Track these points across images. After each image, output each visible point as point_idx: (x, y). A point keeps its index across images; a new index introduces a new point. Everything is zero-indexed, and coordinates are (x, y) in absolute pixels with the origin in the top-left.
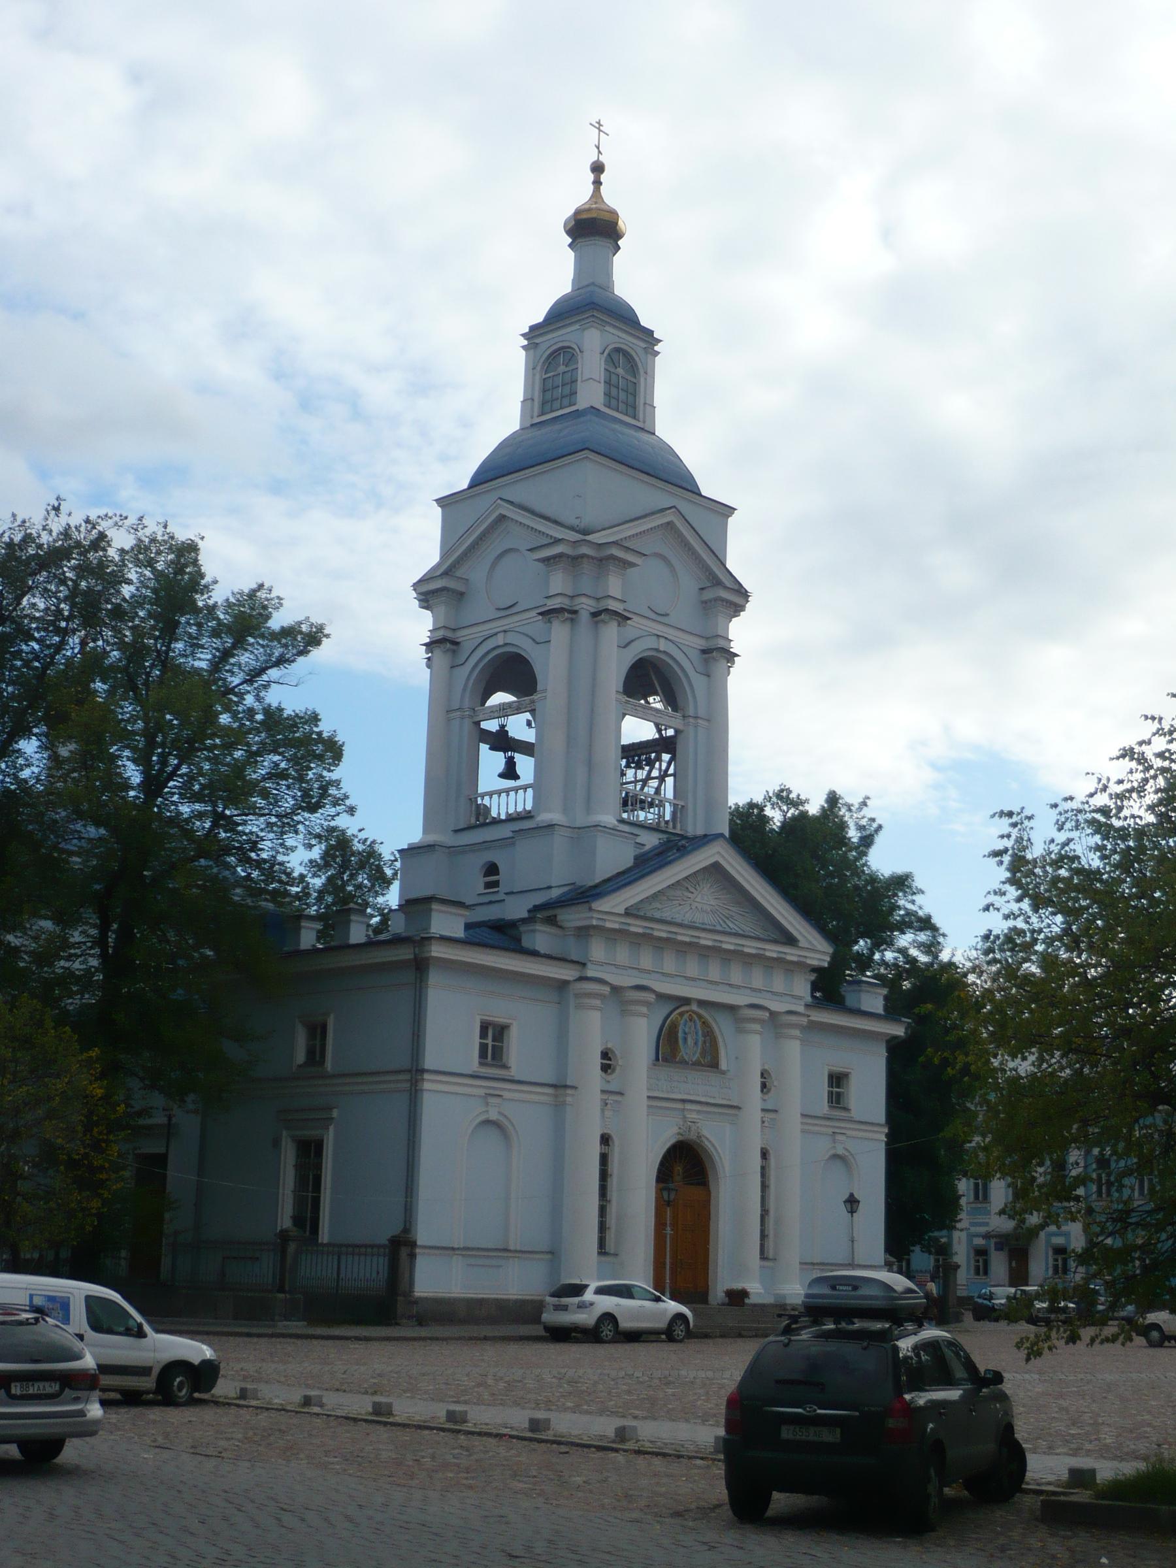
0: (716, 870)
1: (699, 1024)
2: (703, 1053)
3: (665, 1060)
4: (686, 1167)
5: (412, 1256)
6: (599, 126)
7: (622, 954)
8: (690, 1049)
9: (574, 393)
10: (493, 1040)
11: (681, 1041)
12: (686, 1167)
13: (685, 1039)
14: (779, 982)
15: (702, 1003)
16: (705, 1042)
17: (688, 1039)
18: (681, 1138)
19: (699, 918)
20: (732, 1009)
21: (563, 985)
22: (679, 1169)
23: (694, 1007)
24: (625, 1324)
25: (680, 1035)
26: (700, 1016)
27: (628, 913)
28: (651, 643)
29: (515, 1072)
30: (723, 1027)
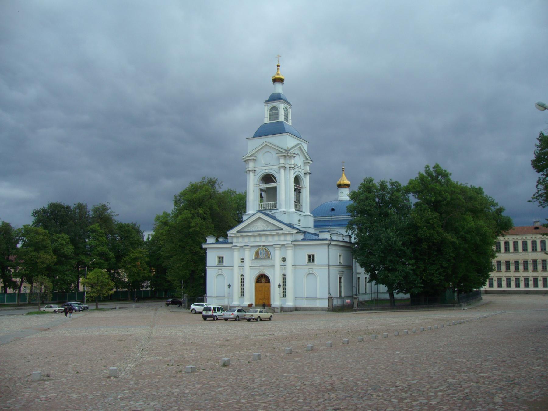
0: (259, 218)
2: (266, 256)
4: (263, 279)
7: (241, 240)
9: (278, 117)
10: (221, 259)
12: (263, 279)
14: (282, 238)
15: (263, 246)
17: (262, 254)
19: (260, 229)
20: (272, 245)
21: (231, 248)
22: (263, 280)
24: (197, 311)
27: (238, 232)
30: (271, 249)
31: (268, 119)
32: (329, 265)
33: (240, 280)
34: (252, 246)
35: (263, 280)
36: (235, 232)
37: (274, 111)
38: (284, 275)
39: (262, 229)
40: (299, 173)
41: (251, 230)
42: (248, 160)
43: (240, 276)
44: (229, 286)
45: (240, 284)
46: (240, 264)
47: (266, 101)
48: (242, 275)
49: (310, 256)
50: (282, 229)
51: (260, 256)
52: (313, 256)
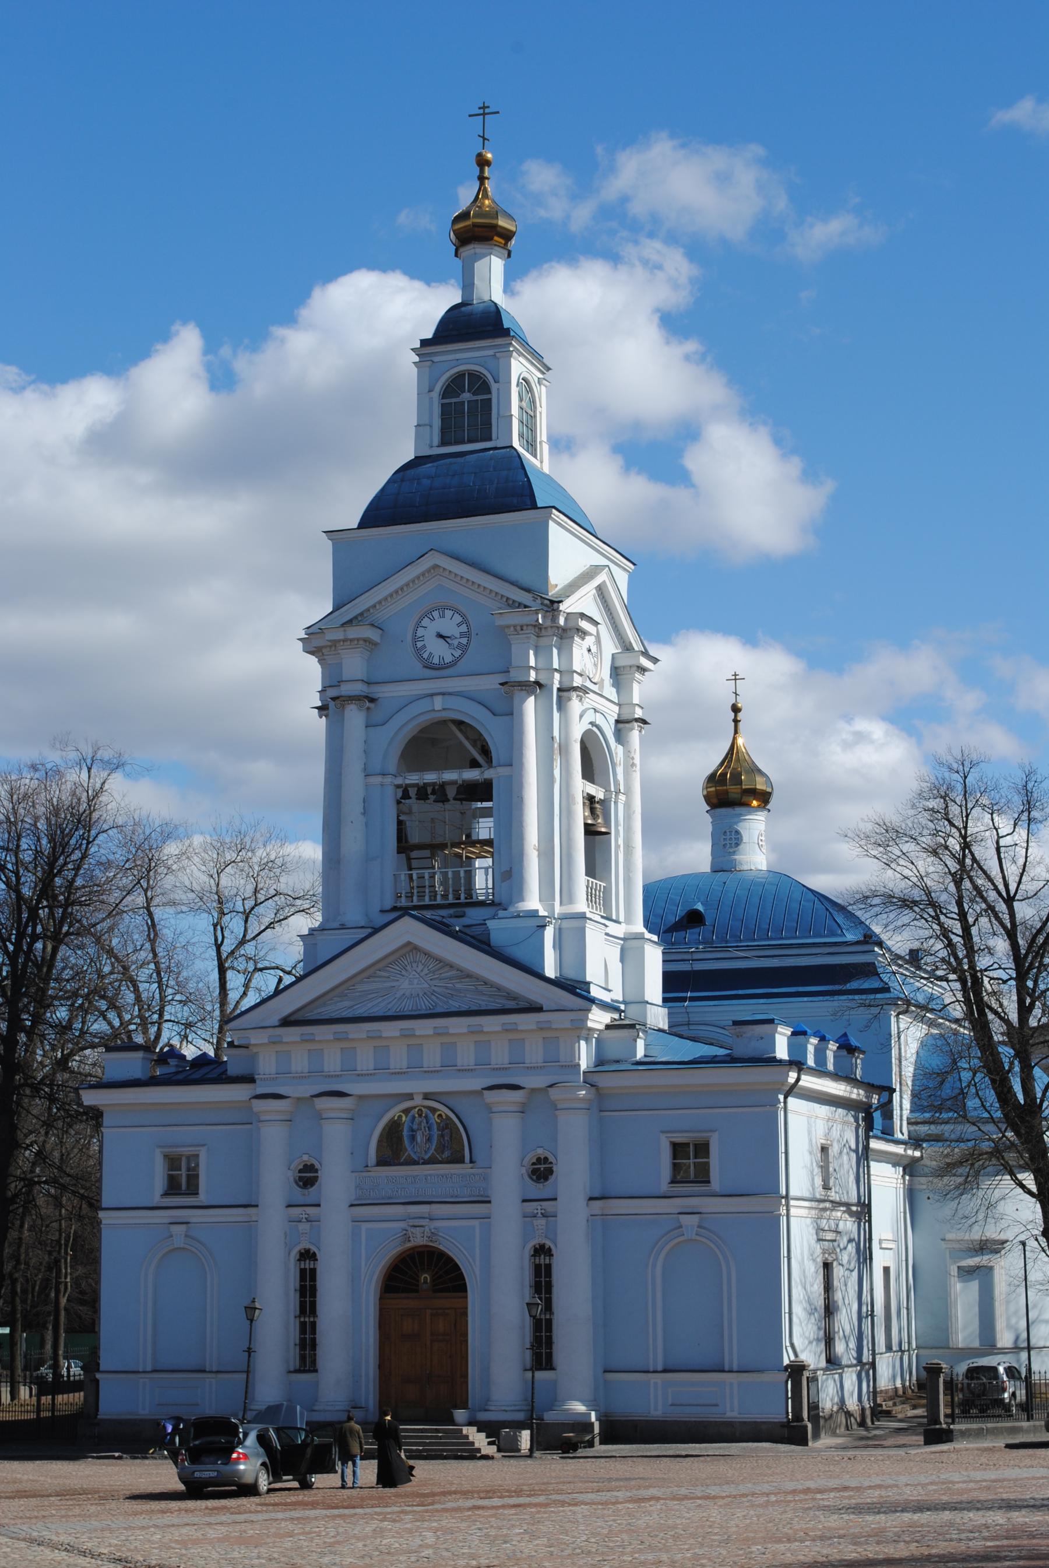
1: (434, 1119)
2: (441, 1148)
3: (381, 1162)
5: (97, 1381)
6: (484, 111)
8: (419, 1145)
11: (405, 1139)
13: (413, 1138)
15: (427, 1096)
16: (442, 1136)
18: (408, 1245)
19: (407, 1007)
23: (418, 1101)
25: (405, 1133)
26: (434, 1110)
27: (287, 1022)
28: (423, 706)
29: (203, 1198)
31: (436, 440)
32: (787, 1197)
33: (294, 1282)
34: (361, 1097)
35: (426, 1277)
36: (275, 1020)
37: (466, 396)
38: (542, 1251)
39: (424, 1006)
40: (600, 720)
41: (360, 1011)
42: (334, 643)
43: (294, 1254)
44: (250, 1311)
45: (294, 1299)
46: (299, 1195)
47: (424, 343)
48: (307, 1255)
49: (678, 1149)
50: (535, 1008)
51: (409, 1150)
52: (702, 1149)
